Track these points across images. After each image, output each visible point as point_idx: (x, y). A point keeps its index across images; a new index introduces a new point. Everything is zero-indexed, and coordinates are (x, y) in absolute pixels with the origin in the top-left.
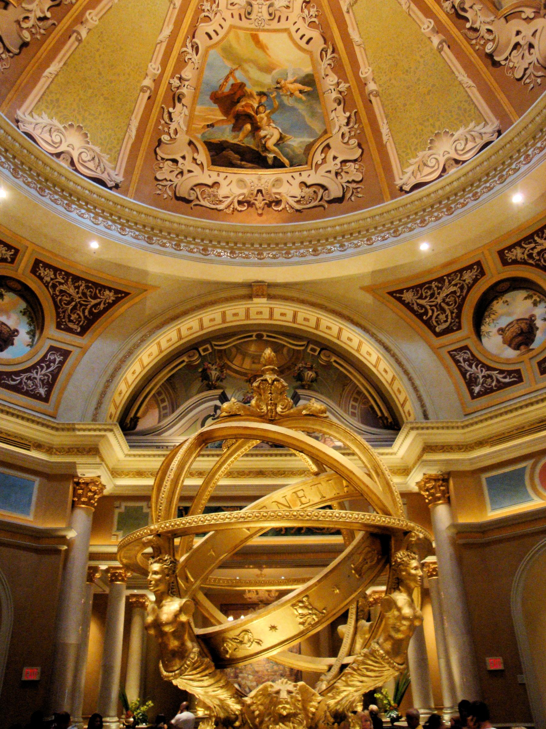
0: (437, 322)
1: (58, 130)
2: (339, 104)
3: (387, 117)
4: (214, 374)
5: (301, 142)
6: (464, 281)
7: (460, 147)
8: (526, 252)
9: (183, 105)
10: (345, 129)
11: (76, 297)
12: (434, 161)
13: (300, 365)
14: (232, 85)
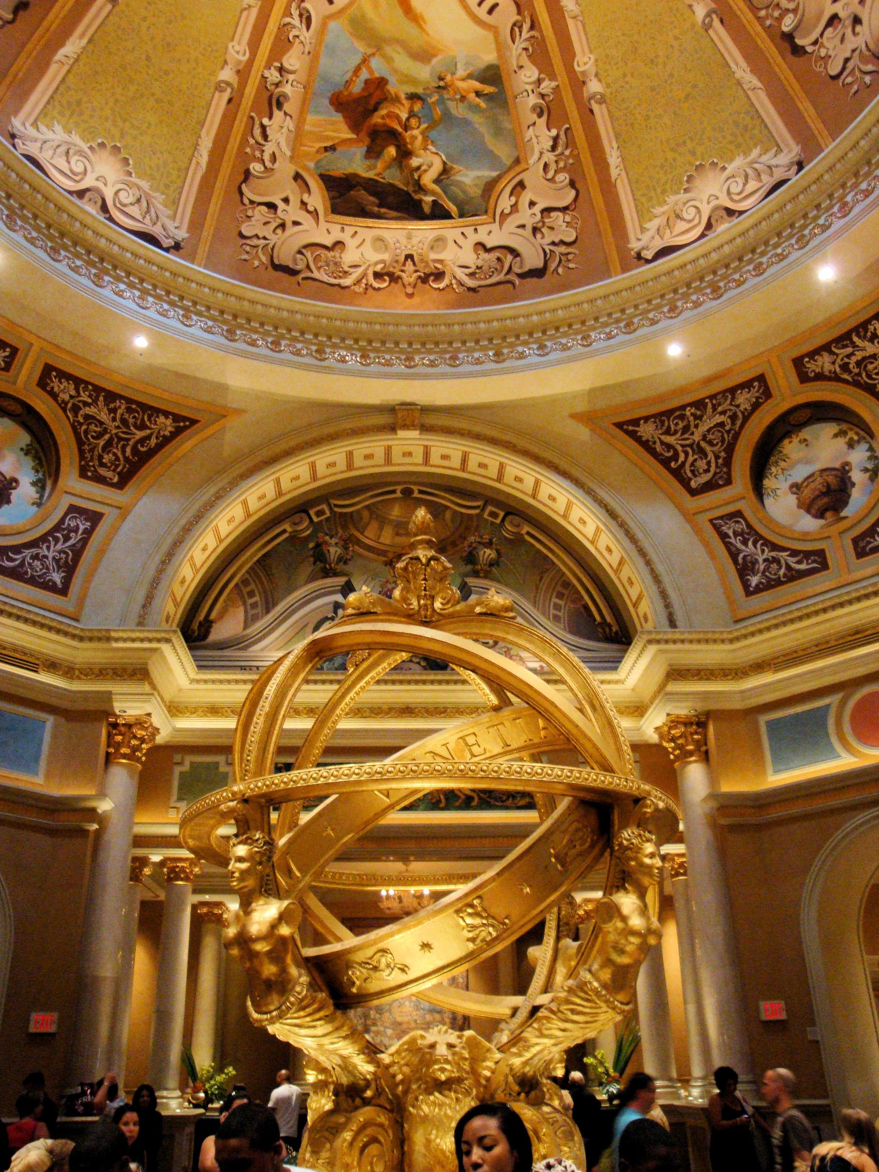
0: (692, 471)
1: (80, 153)
2: (540, 115)
3: (617, 136)
4: (334, 551)
5: (478, 177)
6: (738, 406)
7: (735, 189)
8: (839, 360)
9: (286, 114)
10: (549, 157)
11: (112, 426)
12: (693, 211)
13: (472, 539)
14: (367, 82)
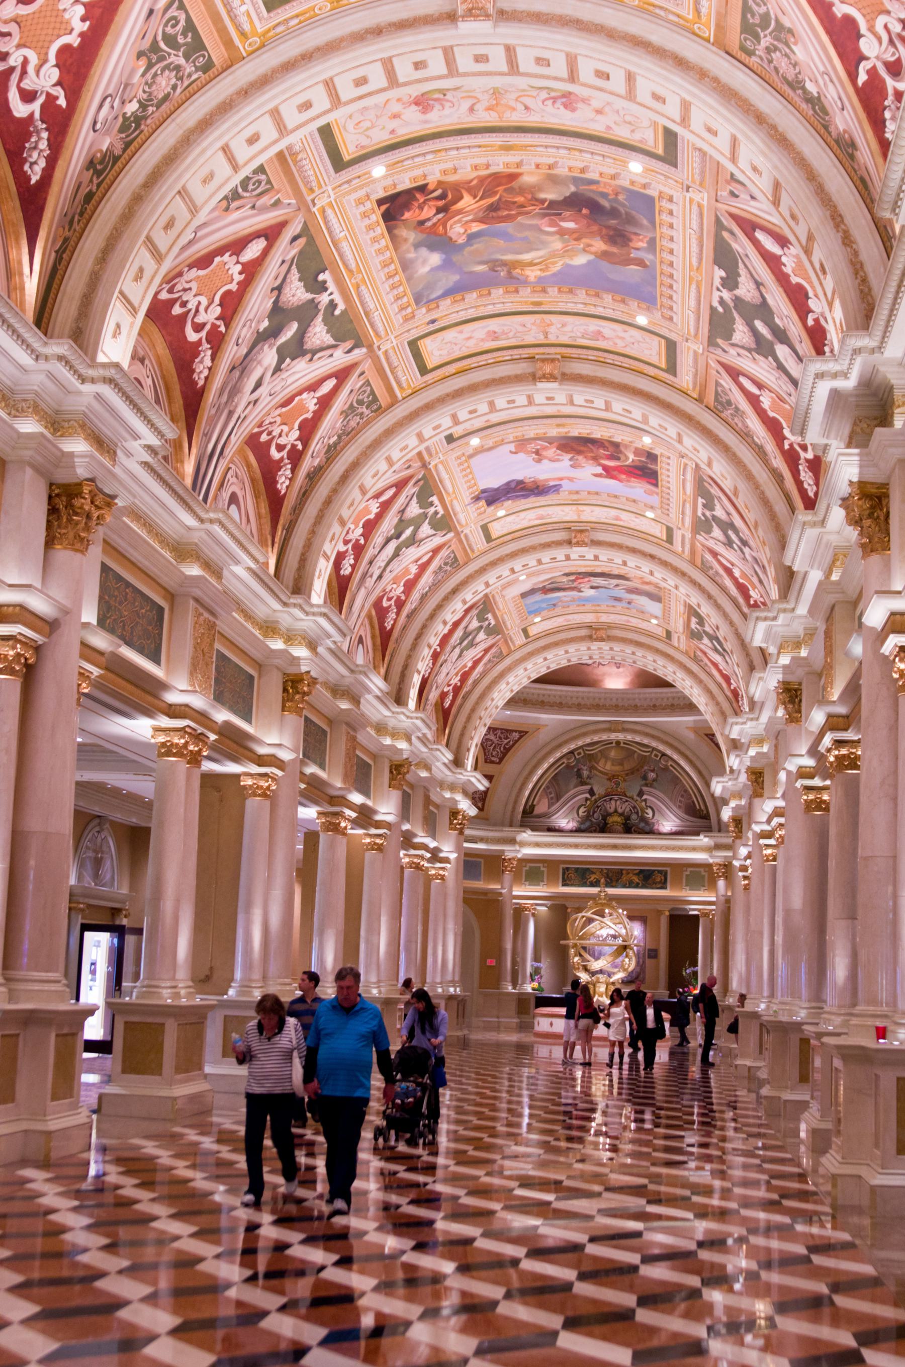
4: (585, 773)
11: (496, 741)
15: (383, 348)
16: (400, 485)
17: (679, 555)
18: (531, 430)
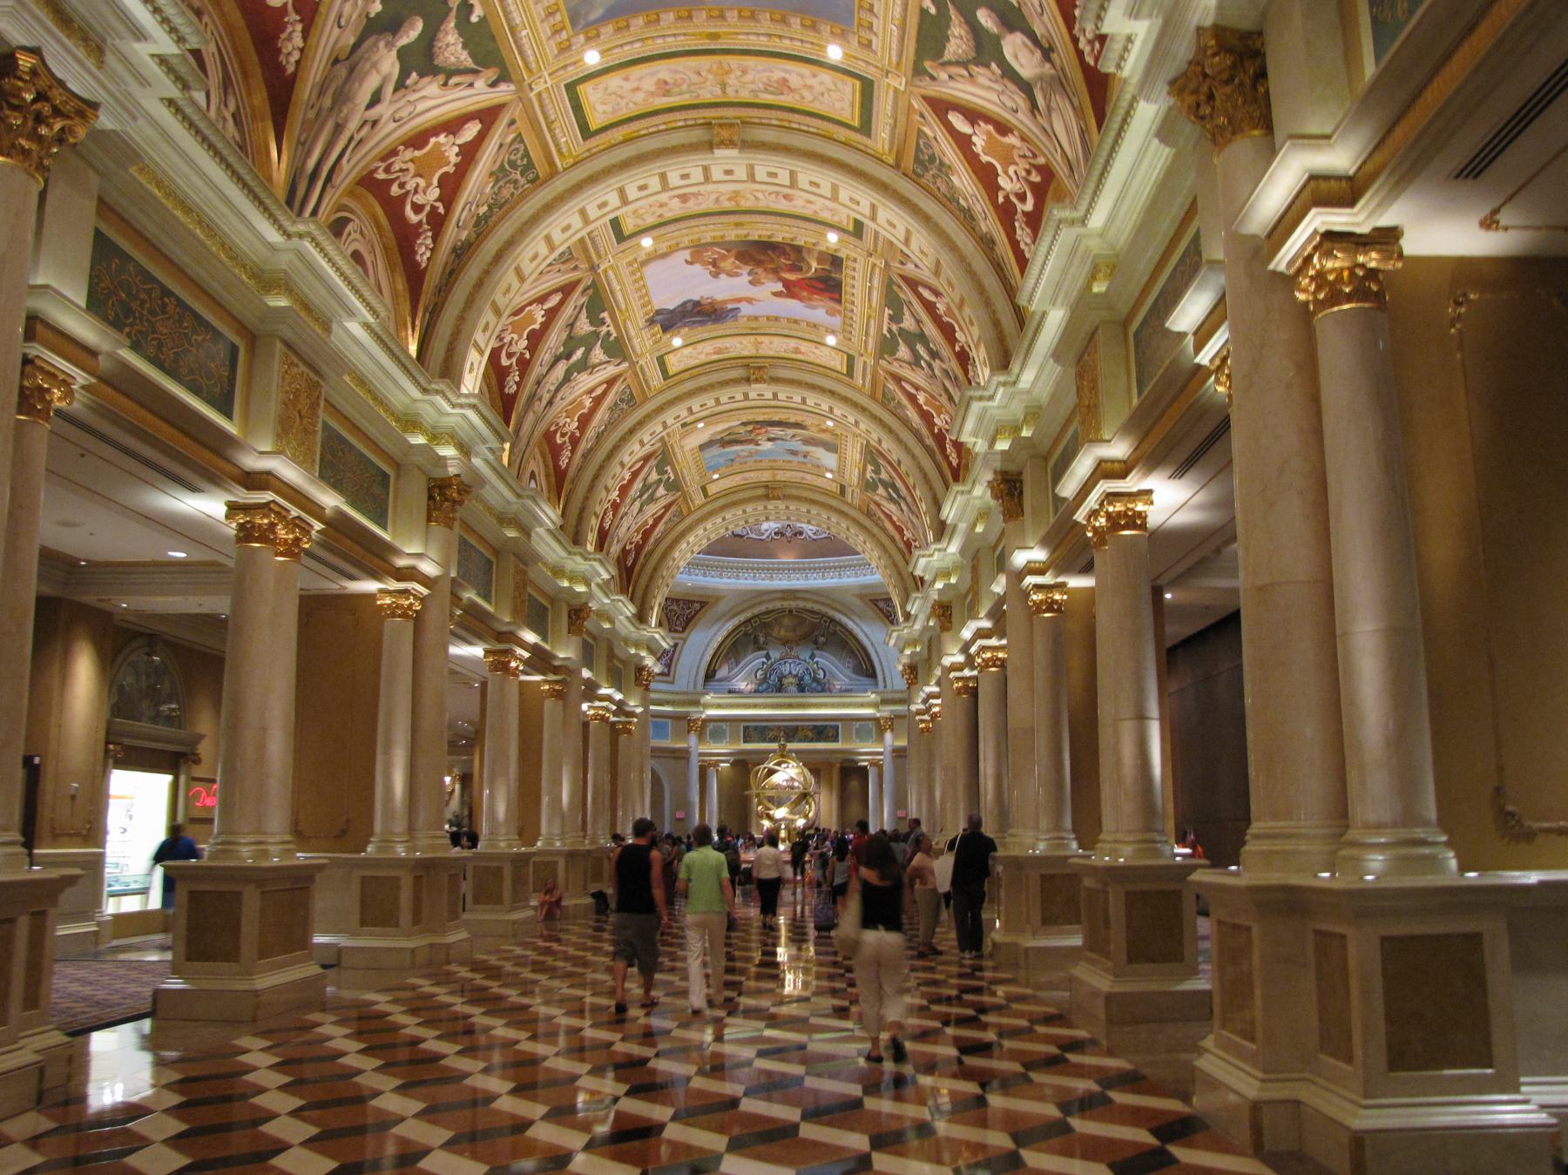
4: (762, 639)
15: (539, 87)
16: (567, 290)
17: (859, 391)
18: (709, 232)
